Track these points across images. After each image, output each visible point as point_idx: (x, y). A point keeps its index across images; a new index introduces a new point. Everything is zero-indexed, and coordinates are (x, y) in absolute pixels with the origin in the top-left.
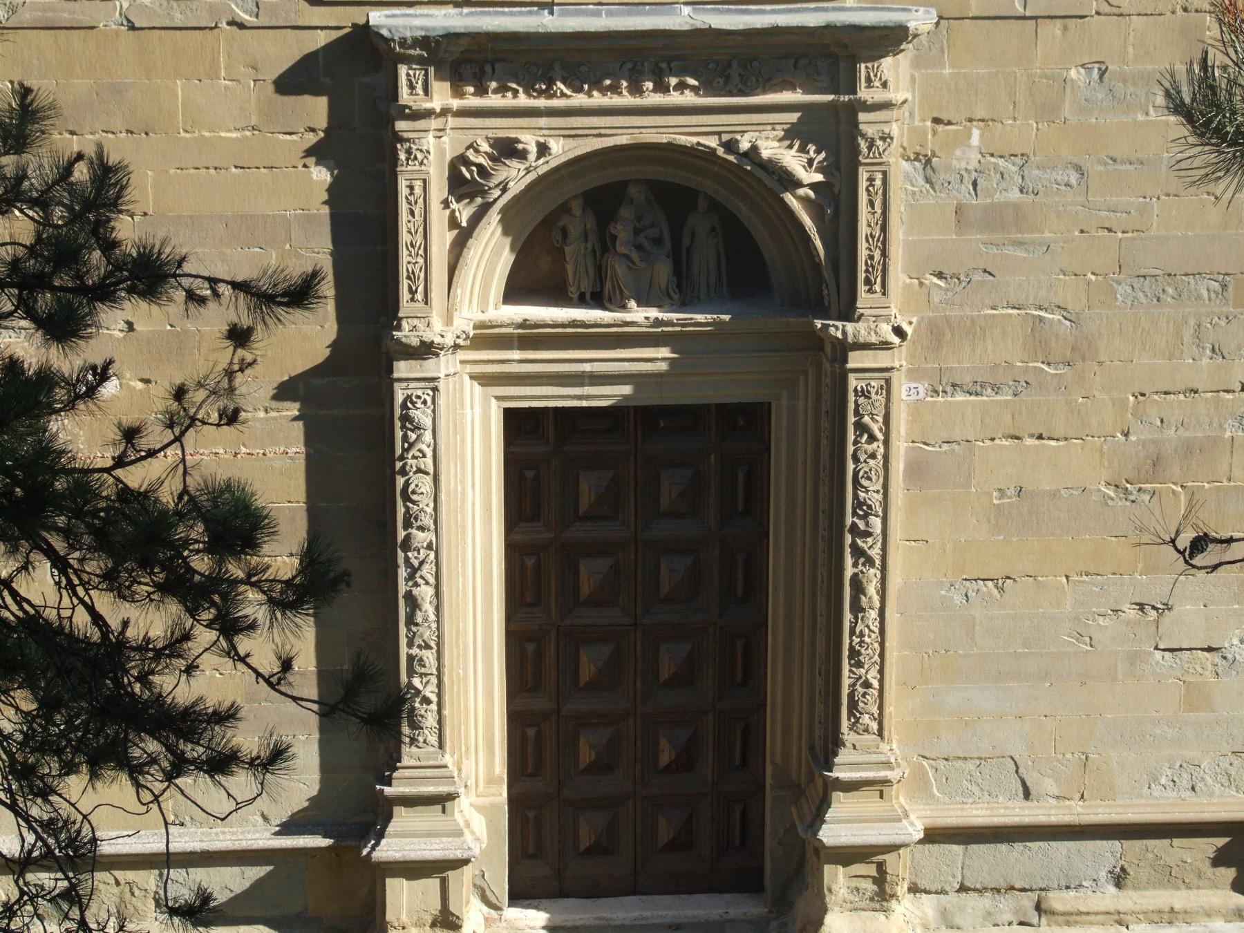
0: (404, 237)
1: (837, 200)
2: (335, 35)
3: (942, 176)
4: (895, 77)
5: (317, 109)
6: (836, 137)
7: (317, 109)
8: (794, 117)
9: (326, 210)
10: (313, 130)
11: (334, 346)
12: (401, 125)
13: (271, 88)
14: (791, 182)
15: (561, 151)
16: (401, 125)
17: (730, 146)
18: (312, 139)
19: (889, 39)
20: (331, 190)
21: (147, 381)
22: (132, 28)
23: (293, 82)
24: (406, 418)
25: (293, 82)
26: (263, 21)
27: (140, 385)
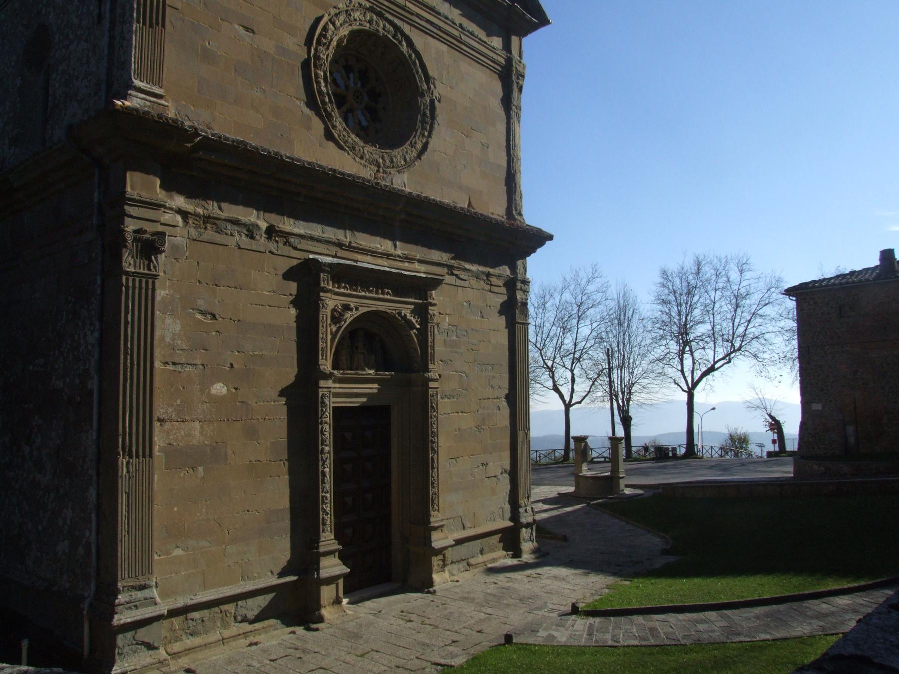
0: (321, 335)
1: (423, 333)
2: (299, 261)
3: (441, 330)
4: (436, 296)
5: (293, 287)
6: (422, 312)
7: (293, 287)
8: (412, 307)
9: (295, 325)
10: (291, 295)
11: (296, 376)
12: (322, 294)
13: (281, 277)
14: (412, 327)
15: (363, 310)
16: (322, 294)
17: (400, 314)
18: (291, 298)
19: (435, 283)
20: (297, 317)
21: (236, 389)
22: (239, 248)
23: (288, 275)
24: (323, 402)
25: (288, 275)
26: (279, 253)
27: (234, 391)
